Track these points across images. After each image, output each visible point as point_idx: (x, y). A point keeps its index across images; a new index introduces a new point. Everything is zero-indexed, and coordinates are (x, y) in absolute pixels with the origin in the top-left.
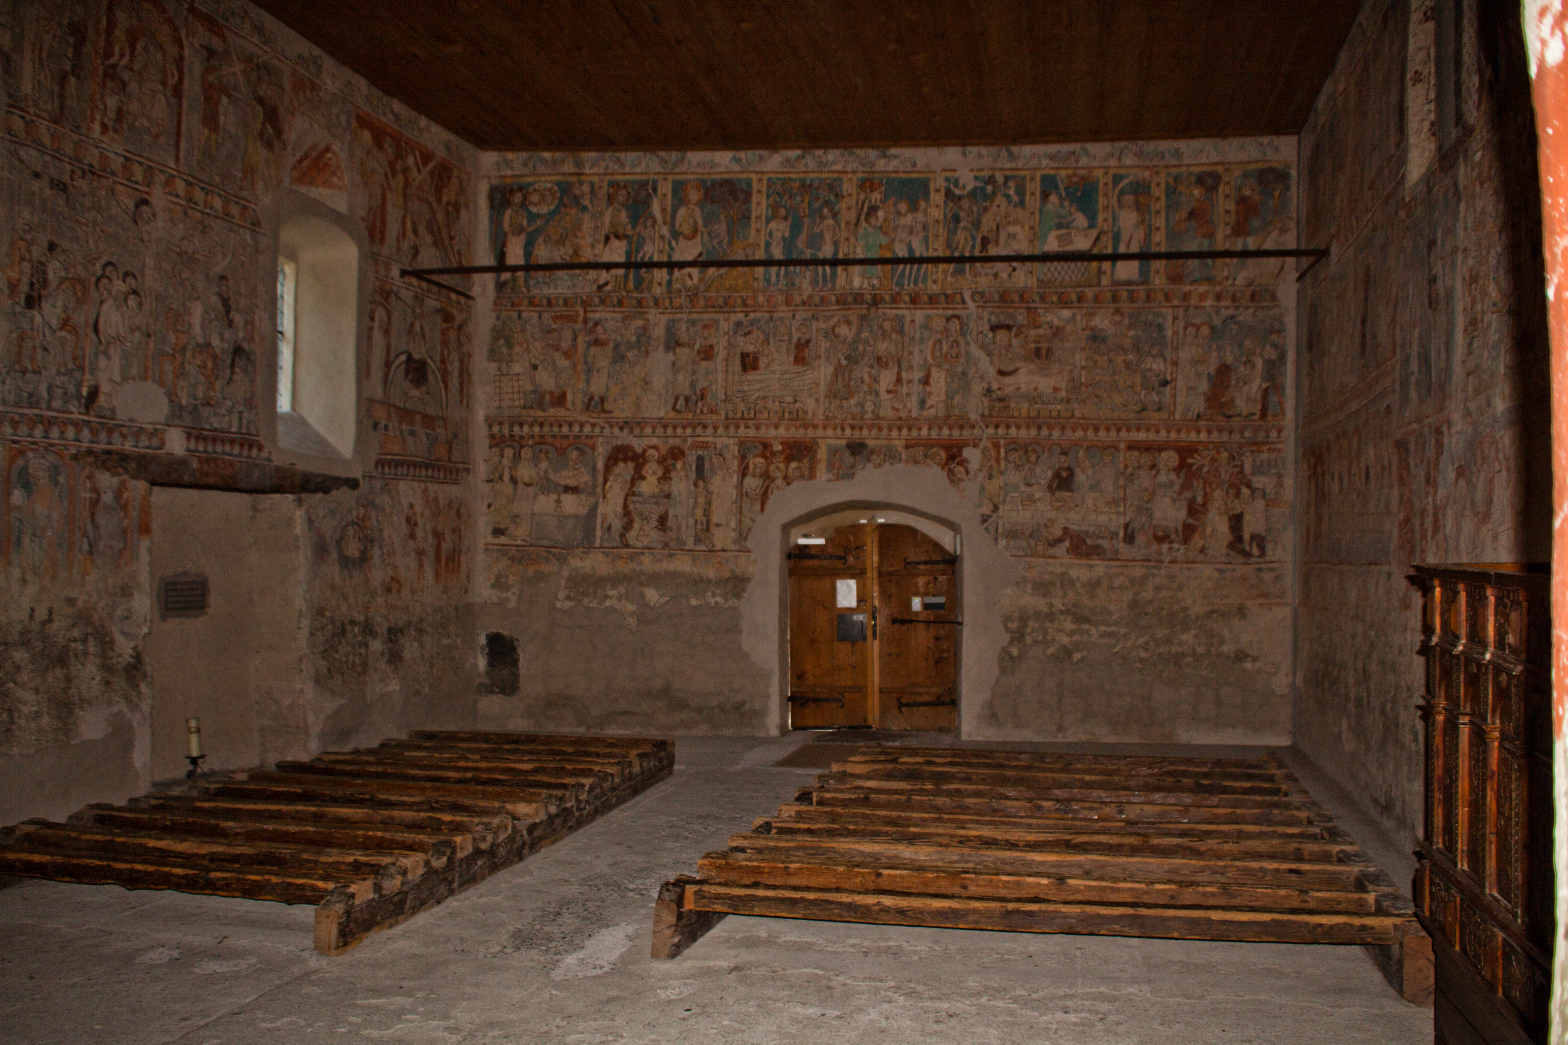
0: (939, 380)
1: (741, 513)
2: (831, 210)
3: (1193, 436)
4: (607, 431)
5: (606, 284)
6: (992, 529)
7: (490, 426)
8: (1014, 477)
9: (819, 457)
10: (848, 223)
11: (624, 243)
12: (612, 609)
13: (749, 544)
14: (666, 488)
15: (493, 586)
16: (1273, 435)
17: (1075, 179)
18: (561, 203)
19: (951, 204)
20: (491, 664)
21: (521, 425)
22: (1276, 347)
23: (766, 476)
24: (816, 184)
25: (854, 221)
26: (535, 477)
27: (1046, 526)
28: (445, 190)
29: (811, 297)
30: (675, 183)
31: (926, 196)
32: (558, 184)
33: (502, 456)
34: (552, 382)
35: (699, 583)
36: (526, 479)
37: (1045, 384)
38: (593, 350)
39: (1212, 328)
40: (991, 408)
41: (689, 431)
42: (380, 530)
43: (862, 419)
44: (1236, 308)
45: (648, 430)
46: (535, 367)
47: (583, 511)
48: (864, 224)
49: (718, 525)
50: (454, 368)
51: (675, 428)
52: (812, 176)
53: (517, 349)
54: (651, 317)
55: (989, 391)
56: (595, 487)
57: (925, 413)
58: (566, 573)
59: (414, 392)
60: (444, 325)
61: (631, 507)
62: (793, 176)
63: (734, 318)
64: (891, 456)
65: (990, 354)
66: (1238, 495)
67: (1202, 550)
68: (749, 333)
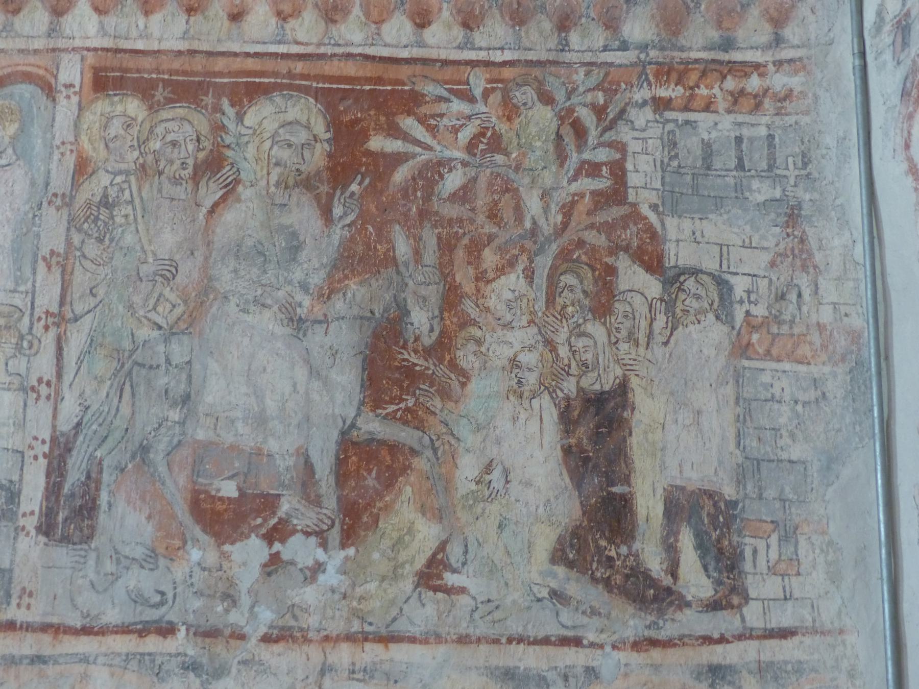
3: (397, 37)
66: (603, 302)
67: (431, 576)
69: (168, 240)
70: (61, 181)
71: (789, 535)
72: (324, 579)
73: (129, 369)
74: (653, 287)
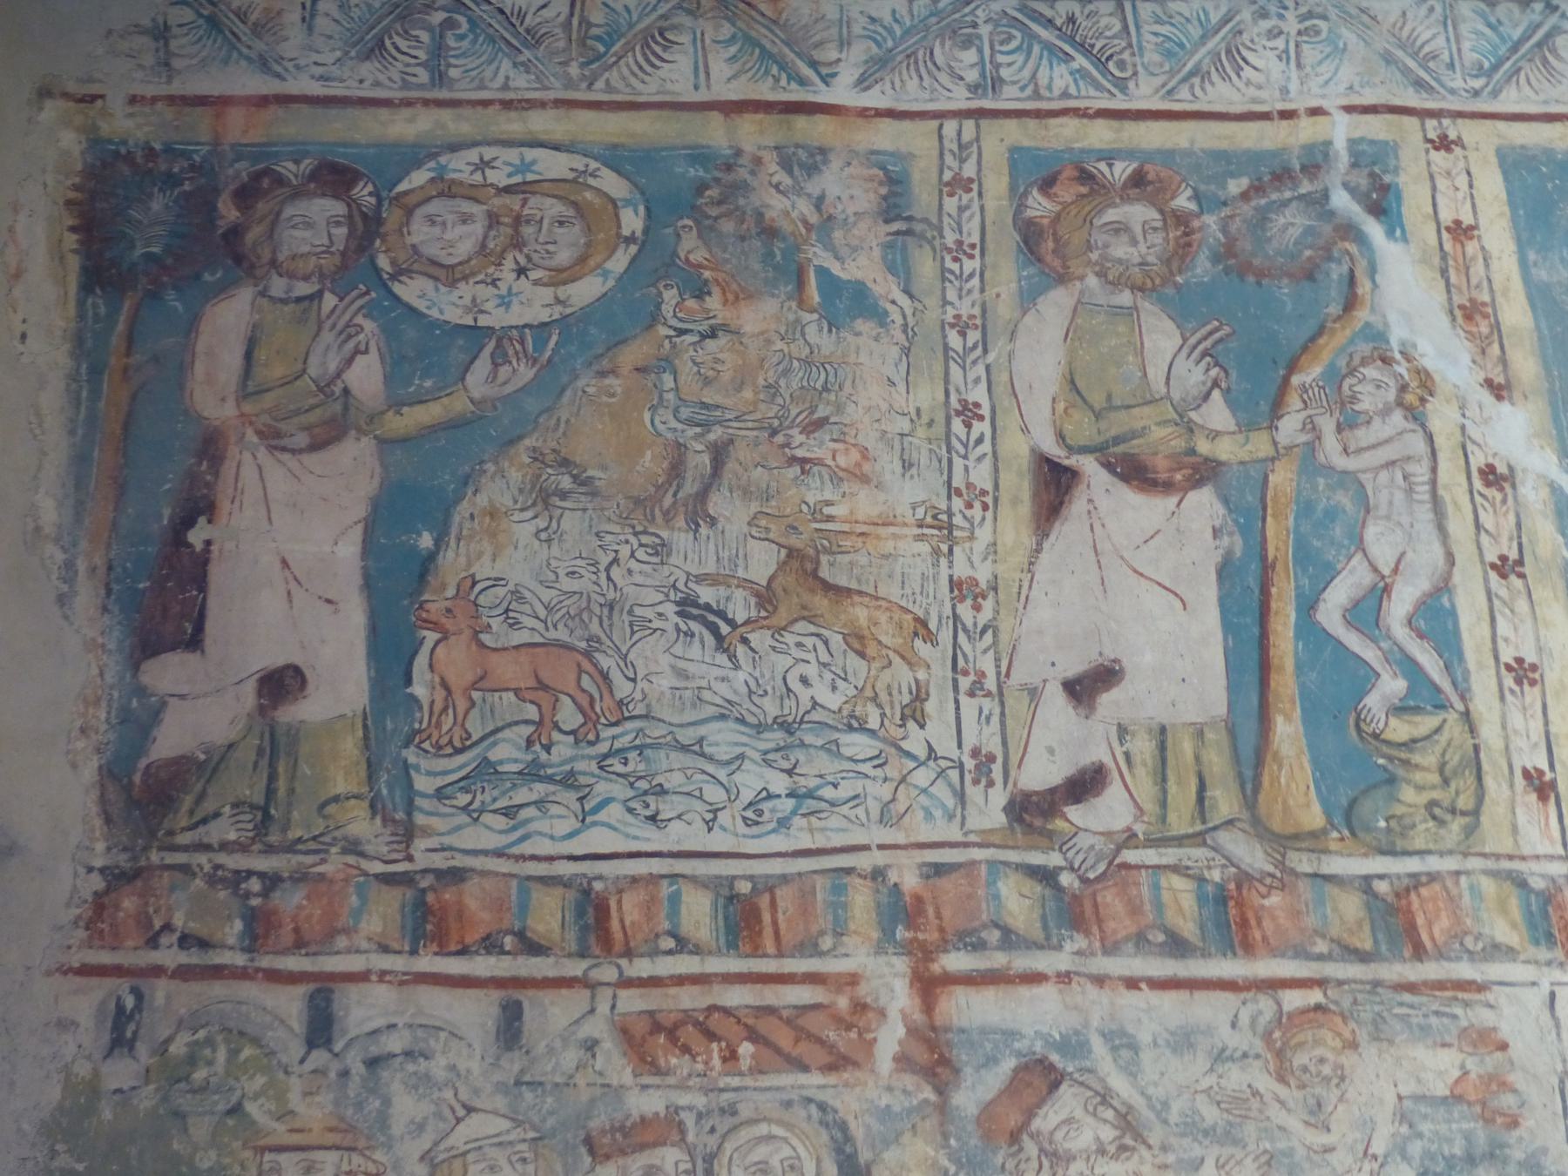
5: (1085, 784)
11: (1203, 504)
18: (656, 261)
30: (1513, 163)
32: (614, 157)
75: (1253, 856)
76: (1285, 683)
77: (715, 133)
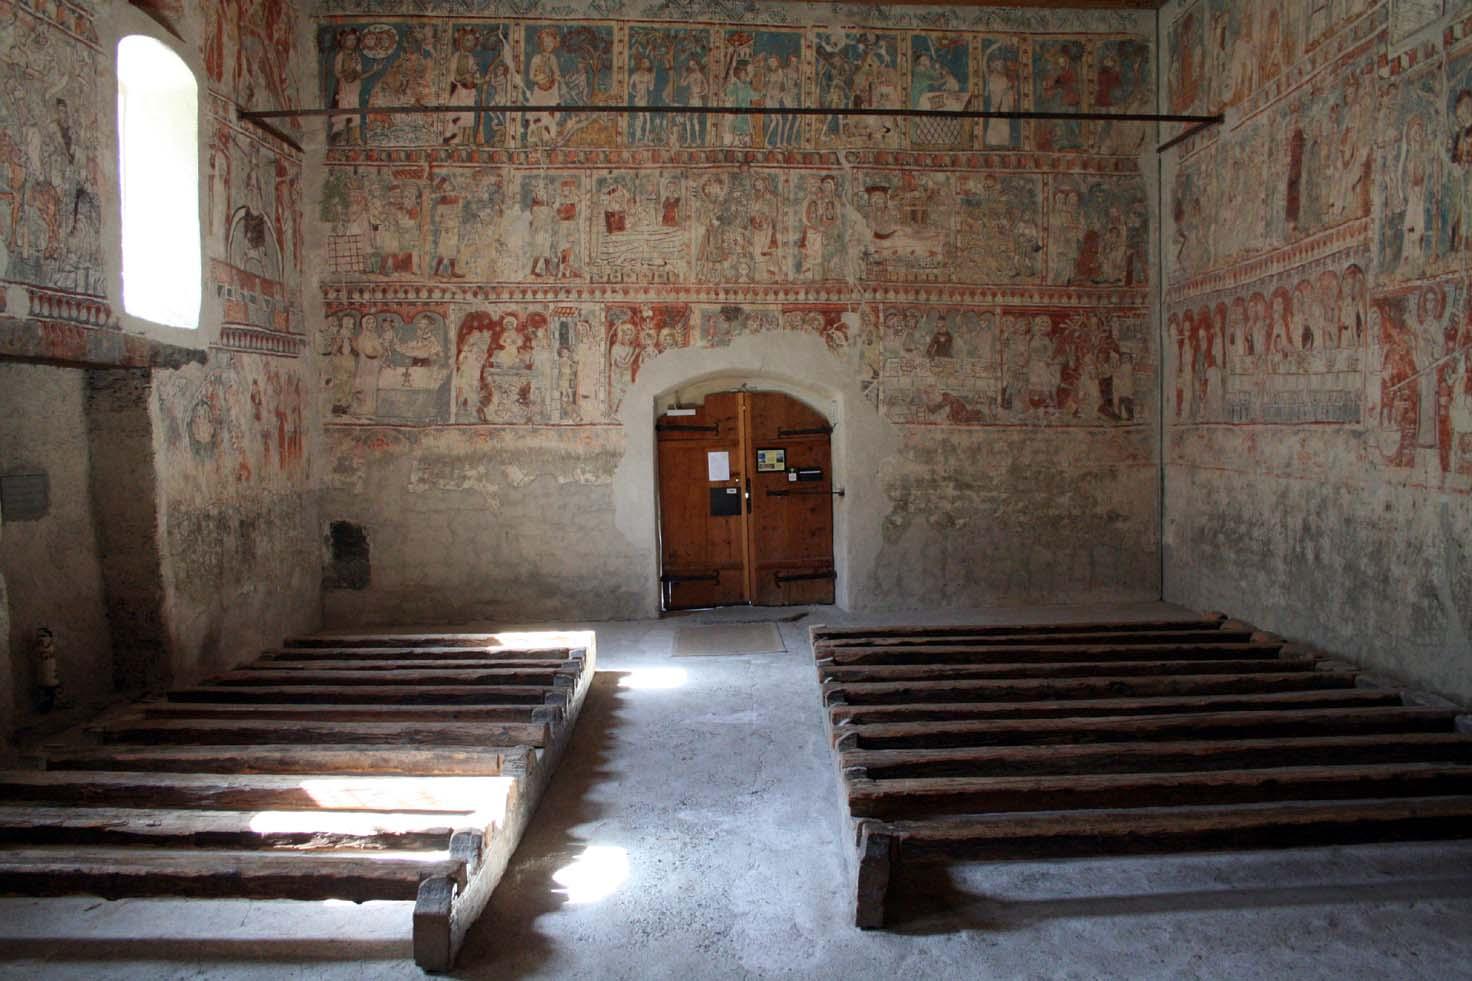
0: (815, 241)
1: (610, 384)
2: (698, 63)
4: (459, 297)
5: (454, 136)
6: (874, 395)
7: (326, 294)
8: (895, 343)
9: (692, 323)
10: (716, 77)
11: (474, 92)
12: (470, 492)
13: (619, 417)
14: (527, 357)
15: (335, 470)
16: (1138, 301)
17: (945, 42)
18: (400, 48)
19: (822, 62)
20: (337, 556)
21: (361, 292)
22: (1140, 215)
23: (636, 343)
24: (681, 34)
25: (723, 75)
26: (379, 348)
27: (926, 392)
28: (275, 27)
29: (678, 154)
30: (528, 28)
31: (797, 52)
32: (395, 26)
33: (341, 326)
34: (395, 244)
35: (569, 459)
36: (369, 351)
37: (920, 248)
38: (441, 209)
39: (1080, 195)
40: (869, 272)
41: (550, 296)
42: (229, 410)
43: (736, 282)
44: (1102, 176)
45: (505, 296)
46: (376, 228)
47: (435, 386)
48: (733, 79)
49: (585, 397)
50: (288, 228)
51: (535, 293)
52: (676, 26)
53: (354, 208)
54: (504, 172)
55: (866, 254)
56: (447, 358)
57: (802, 277)
58: (418, 453)
59: (253, 253)
60: (278, 179)
61: (490, 378)
62: (656, 26)
63: (597, 174)
64: (765, 320)
65: (866, 216)
66: (1107, 359)
67: (1076, 413)
68: (614, 190)
69: (1022, 348)
70: (997, 332)
71: (1142, 405)
72: (1055, 415)
73: (1017, 375)
74: (1117, 356)
75: (474, 148)
76: (482, 121)
77: (410, 21)
